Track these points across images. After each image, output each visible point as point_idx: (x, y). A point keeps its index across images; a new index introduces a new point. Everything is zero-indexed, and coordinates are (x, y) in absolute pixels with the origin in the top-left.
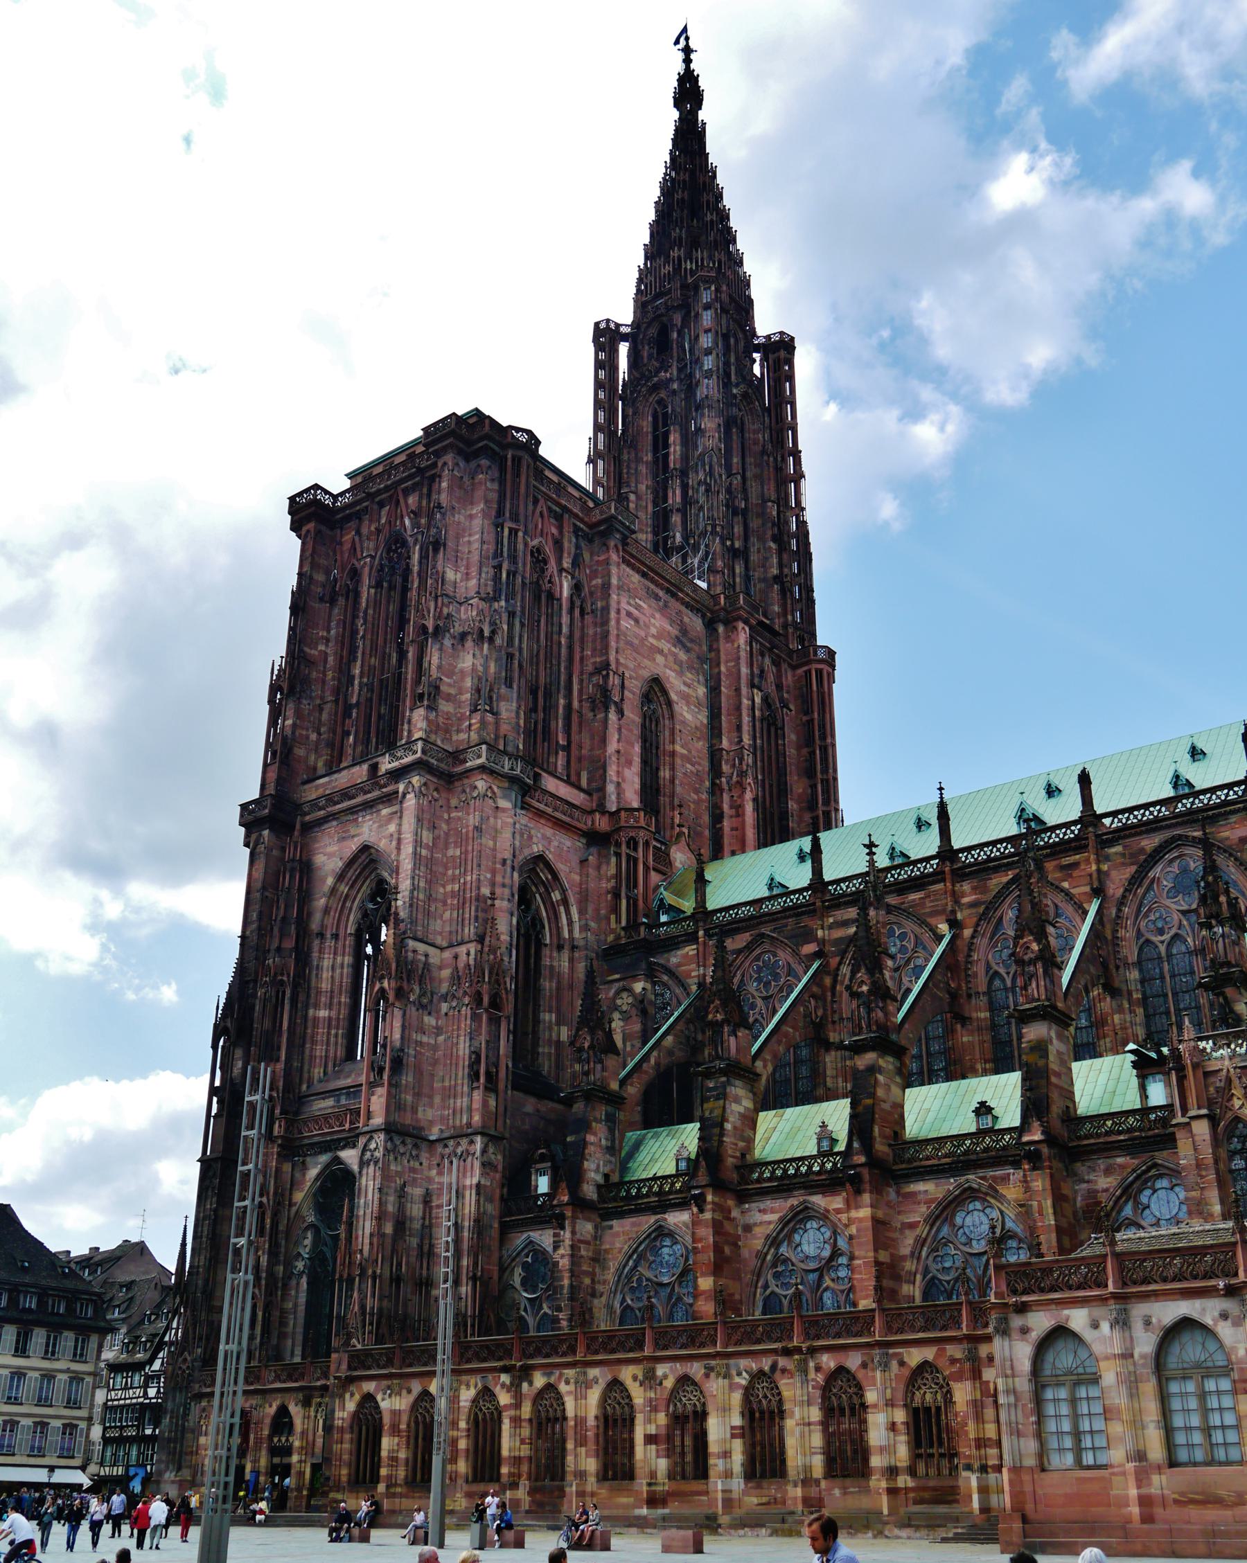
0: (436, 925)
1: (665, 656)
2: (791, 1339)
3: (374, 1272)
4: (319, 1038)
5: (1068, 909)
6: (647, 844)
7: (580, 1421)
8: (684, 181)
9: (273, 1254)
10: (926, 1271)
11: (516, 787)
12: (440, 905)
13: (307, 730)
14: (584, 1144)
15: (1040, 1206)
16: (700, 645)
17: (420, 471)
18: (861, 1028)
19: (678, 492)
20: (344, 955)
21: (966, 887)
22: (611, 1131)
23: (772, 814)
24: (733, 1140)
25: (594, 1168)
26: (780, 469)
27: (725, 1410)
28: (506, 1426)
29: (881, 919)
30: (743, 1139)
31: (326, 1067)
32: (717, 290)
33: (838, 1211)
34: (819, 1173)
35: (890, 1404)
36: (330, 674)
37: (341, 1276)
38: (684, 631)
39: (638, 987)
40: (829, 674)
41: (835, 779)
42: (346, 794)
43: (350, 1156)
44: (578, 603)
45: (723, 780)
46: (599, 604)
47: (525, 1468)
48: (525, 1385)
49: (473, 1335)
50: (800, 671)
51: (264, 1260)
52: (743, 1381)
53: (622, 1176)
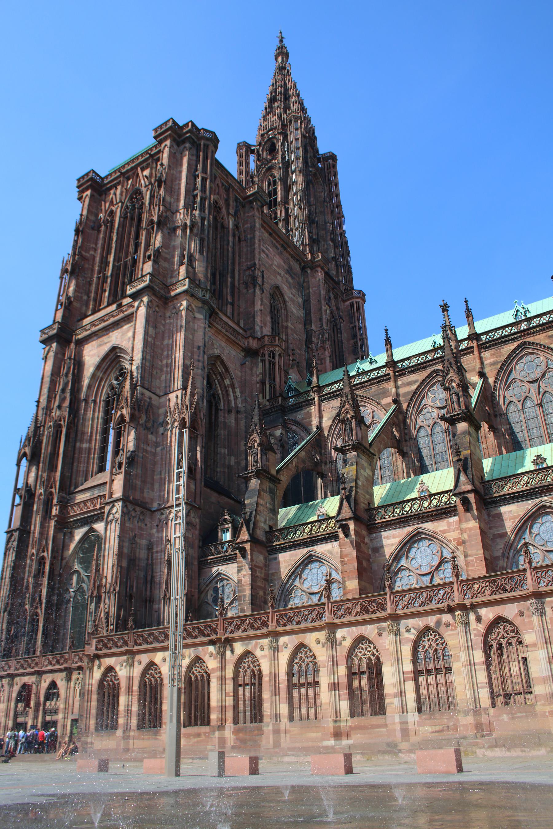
1: (282, 277)
4: (82, 459)
6: (280, 356)
7: (275, 676)
11: (206, 307)
12: (159, 371)
17: (151, 156)
21: (486, 354)
26: (332, 211)
33: (444, 532)
39: (278, 432)
43: (99, 526)
46: (249, 236)
48: (228, 653)
50: (348, 303)
52: (412, 636)
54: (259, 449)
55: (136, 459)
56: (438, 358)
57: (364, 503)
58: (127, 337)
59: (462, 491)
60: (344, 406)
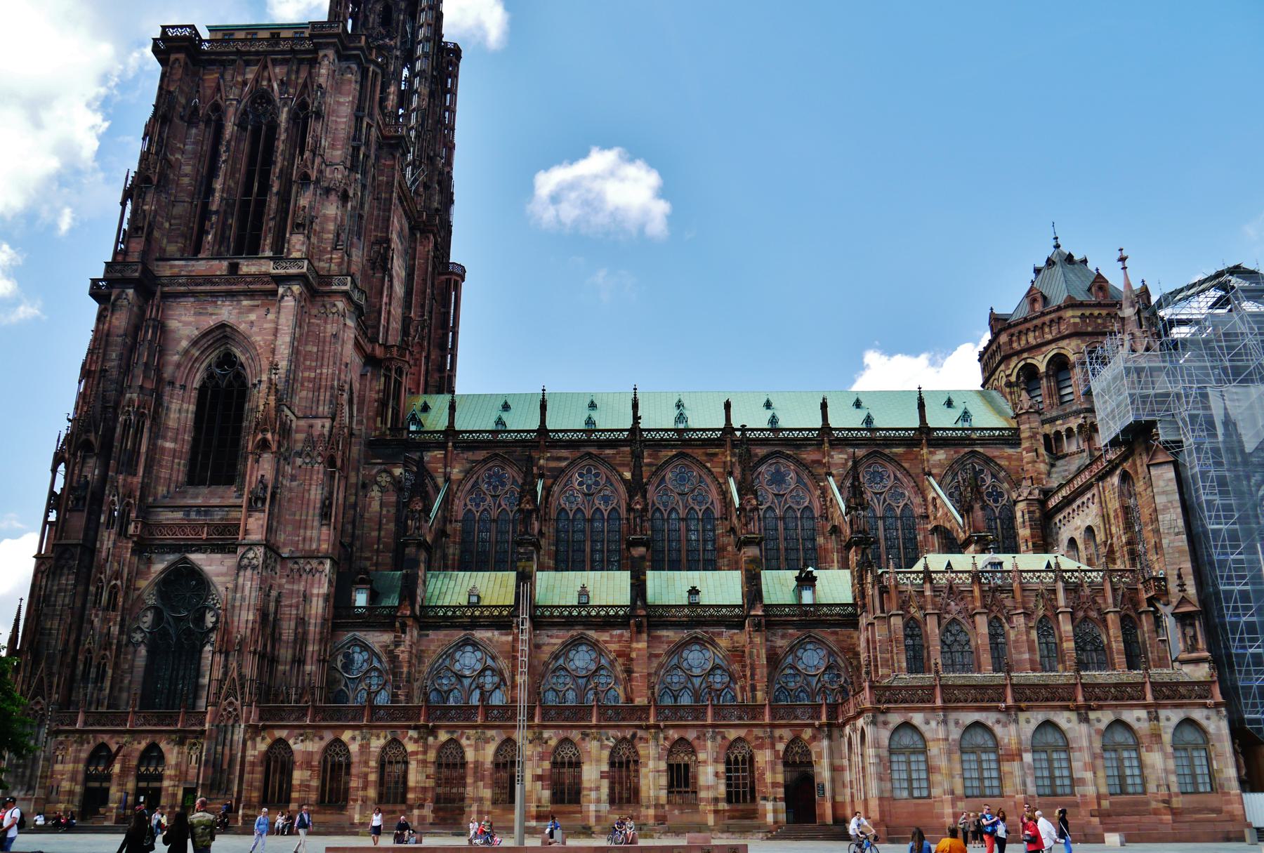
0: (296, 400)
2: (419, 721)
4: (164, 463)
27: (599, 761)
28: (413, 766)
31: (169, 486)
33: (606, 642)
34: (595, 616)
35: (716, 761)
39: (398, 471)
42: (208, 279)
47: (430, 795)
48: (431, 739)
49: (320, 700)
51: (115, 630)
52: (611, 743)
56: (594, 441)
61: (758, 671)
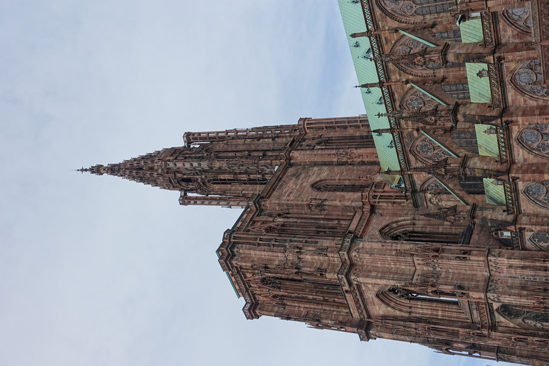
1: (303, 182)
3: (542, 299)
5: (403, 40)
6: (375, 192)
8: (129, 172)
9: (534, 335)
10: (542, 96)
11: (355, 241)
12: (399, 270)
13: (332, 315)
14: (491, 220)
15: (518, 56)
16: (299, 169)
17: (238, 272)
18: (448, 119)
19: (242, 176)
20: (418, 305)
21: (393, 78)
22: (486, 209)
23: (361, 142)
24: (491, 165)
25: (501, 216)
26: (233, 138)
29: (407, 112)
30: (490, 162)
32: (169, 161)
33: (519, 128)
36: (312, 306)
37: (543, 311)
38: (294, 175)
39: (429, 196)
40: (308, 121)
41: (348, 118)
42: (357, 302)
43: (496, 306)
44: (285, 215)
45: (349, 161)
46: (285, 207)
50: (307, 131)
51: (537, 339)
53: (504, 205)
54: (456, 216)
55: (459, 285)
57: (497, 165)
58: (371, 288)
59: (500, 123)
60: (437, 172)
61: (531, 56)
